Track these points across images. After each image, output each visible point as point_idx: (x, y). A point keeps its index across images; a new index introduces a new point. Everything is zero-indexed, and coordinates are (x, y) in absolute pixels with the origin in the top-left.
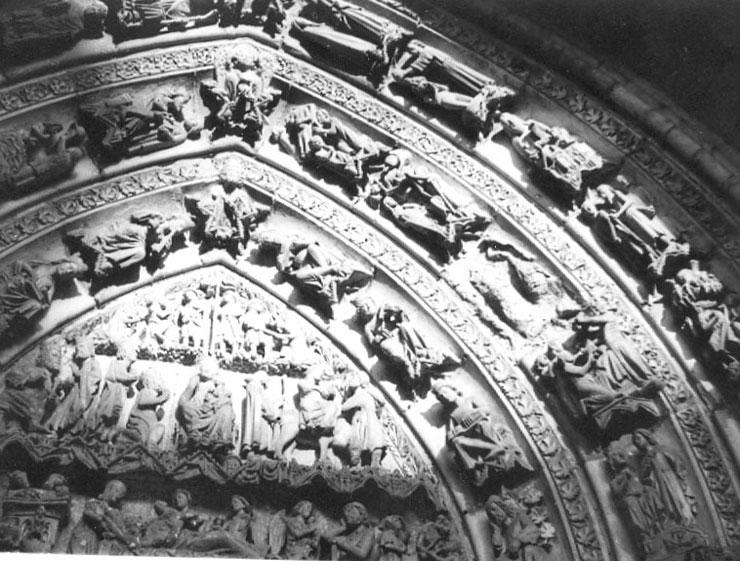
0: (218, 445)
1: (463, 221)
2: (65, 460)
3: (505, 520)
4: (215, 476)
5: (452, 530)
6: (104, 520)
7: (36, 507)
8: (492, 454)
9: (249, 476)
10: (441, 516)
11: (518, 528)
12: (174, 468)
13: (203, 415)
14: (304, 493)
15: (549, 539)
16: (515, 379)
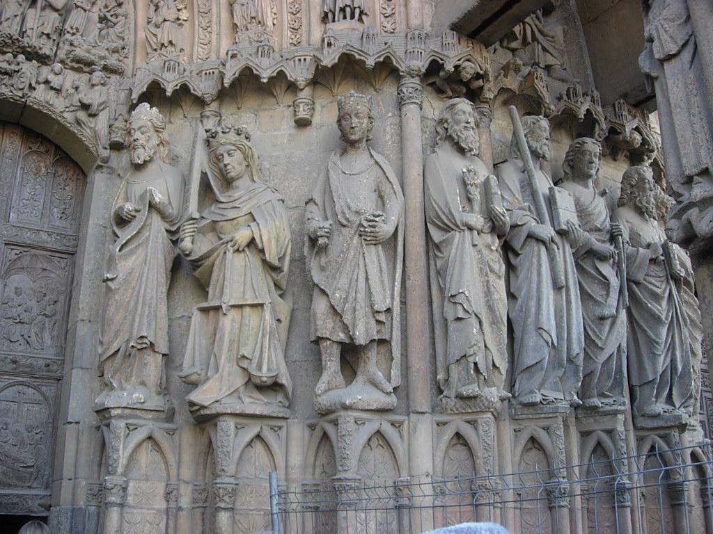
11: (165, 9)
15: (184, 20)
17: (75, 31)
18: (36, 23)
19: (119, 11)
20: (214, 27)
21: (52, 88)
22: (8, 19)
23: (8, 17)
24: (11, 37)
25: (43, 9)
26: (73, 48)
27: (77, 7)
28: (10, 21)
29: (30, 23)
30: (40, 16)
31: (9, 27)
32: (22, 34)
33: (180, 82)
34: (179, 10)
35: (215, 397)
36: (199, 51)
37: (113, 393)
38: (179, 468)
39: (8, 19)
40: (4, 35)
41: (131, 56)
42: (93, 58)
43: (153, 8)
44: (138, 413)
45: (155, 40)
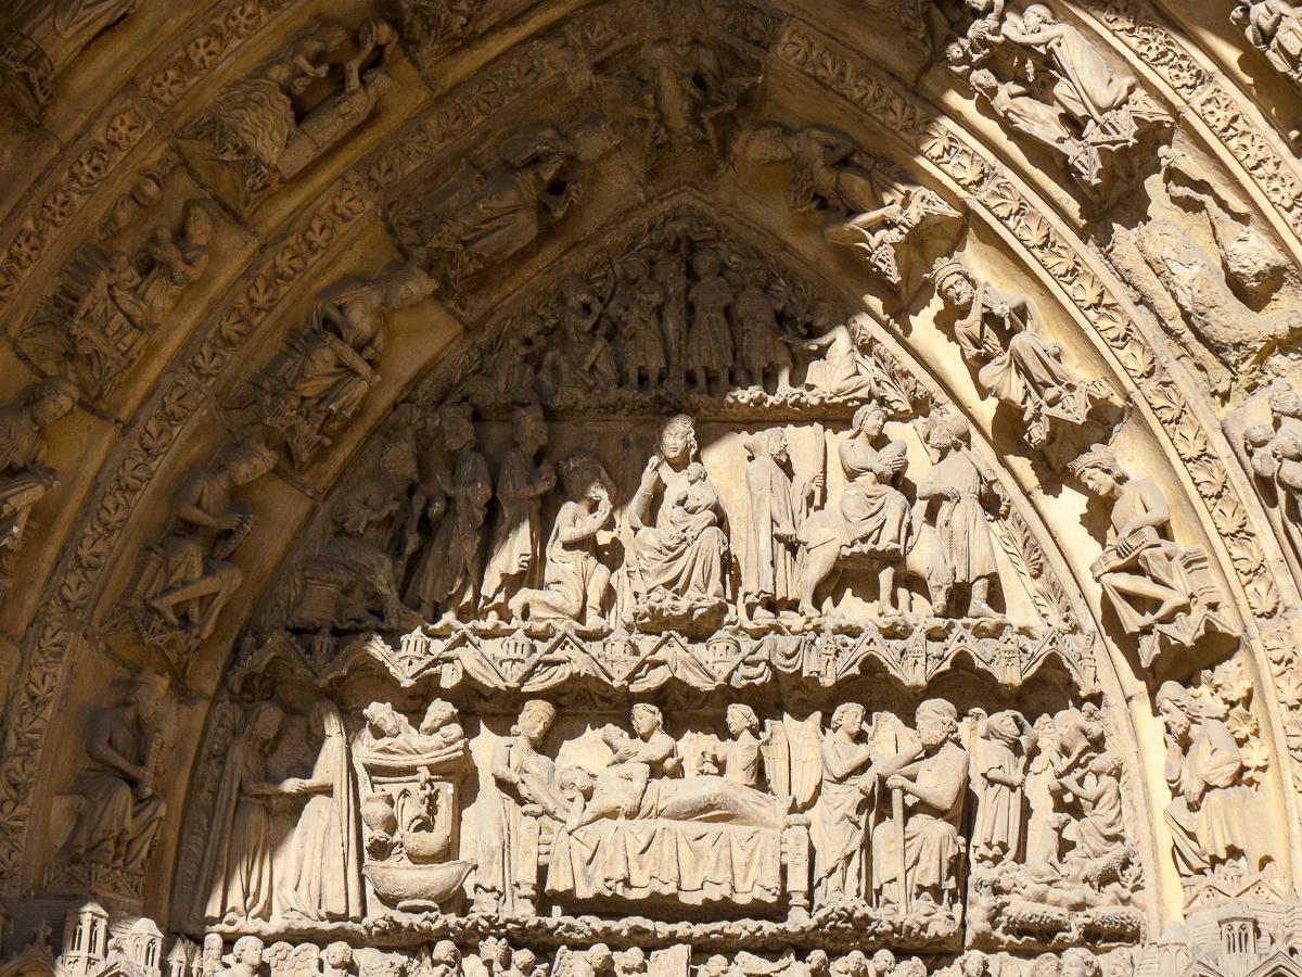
0: (700, 611)
1: (1113, 143)
2: (449, 678)
3: (1188, 729)
4: (695, 680)
5: (1111, 728)
6: (523, 782)
7: (412, 770)
8: (1162, 611)
9: (752, 671)
10: (1089, 706)
12: (627, 672)
13: (672, 555)
14: (846, 690)
16: (1211, 457)
17: (997, 850)
18: (900, 862)
19: (1099, 762)
22: (834, 870)
23: (831, 865)
24: (851, 915)
25: (909, 812)
26: (1004, 898)
27: (992, 782)
28: (837, 875)
29: (887, 864)
30: (905, 840)
31: (838, 889)
32: (872, 895)
34: (1241, 743)
39: (834, 870)
40: (834, 915)
41: (1149, 880)
42: (1053, 913)
43: (1179, 749)
45: (1194, 845)
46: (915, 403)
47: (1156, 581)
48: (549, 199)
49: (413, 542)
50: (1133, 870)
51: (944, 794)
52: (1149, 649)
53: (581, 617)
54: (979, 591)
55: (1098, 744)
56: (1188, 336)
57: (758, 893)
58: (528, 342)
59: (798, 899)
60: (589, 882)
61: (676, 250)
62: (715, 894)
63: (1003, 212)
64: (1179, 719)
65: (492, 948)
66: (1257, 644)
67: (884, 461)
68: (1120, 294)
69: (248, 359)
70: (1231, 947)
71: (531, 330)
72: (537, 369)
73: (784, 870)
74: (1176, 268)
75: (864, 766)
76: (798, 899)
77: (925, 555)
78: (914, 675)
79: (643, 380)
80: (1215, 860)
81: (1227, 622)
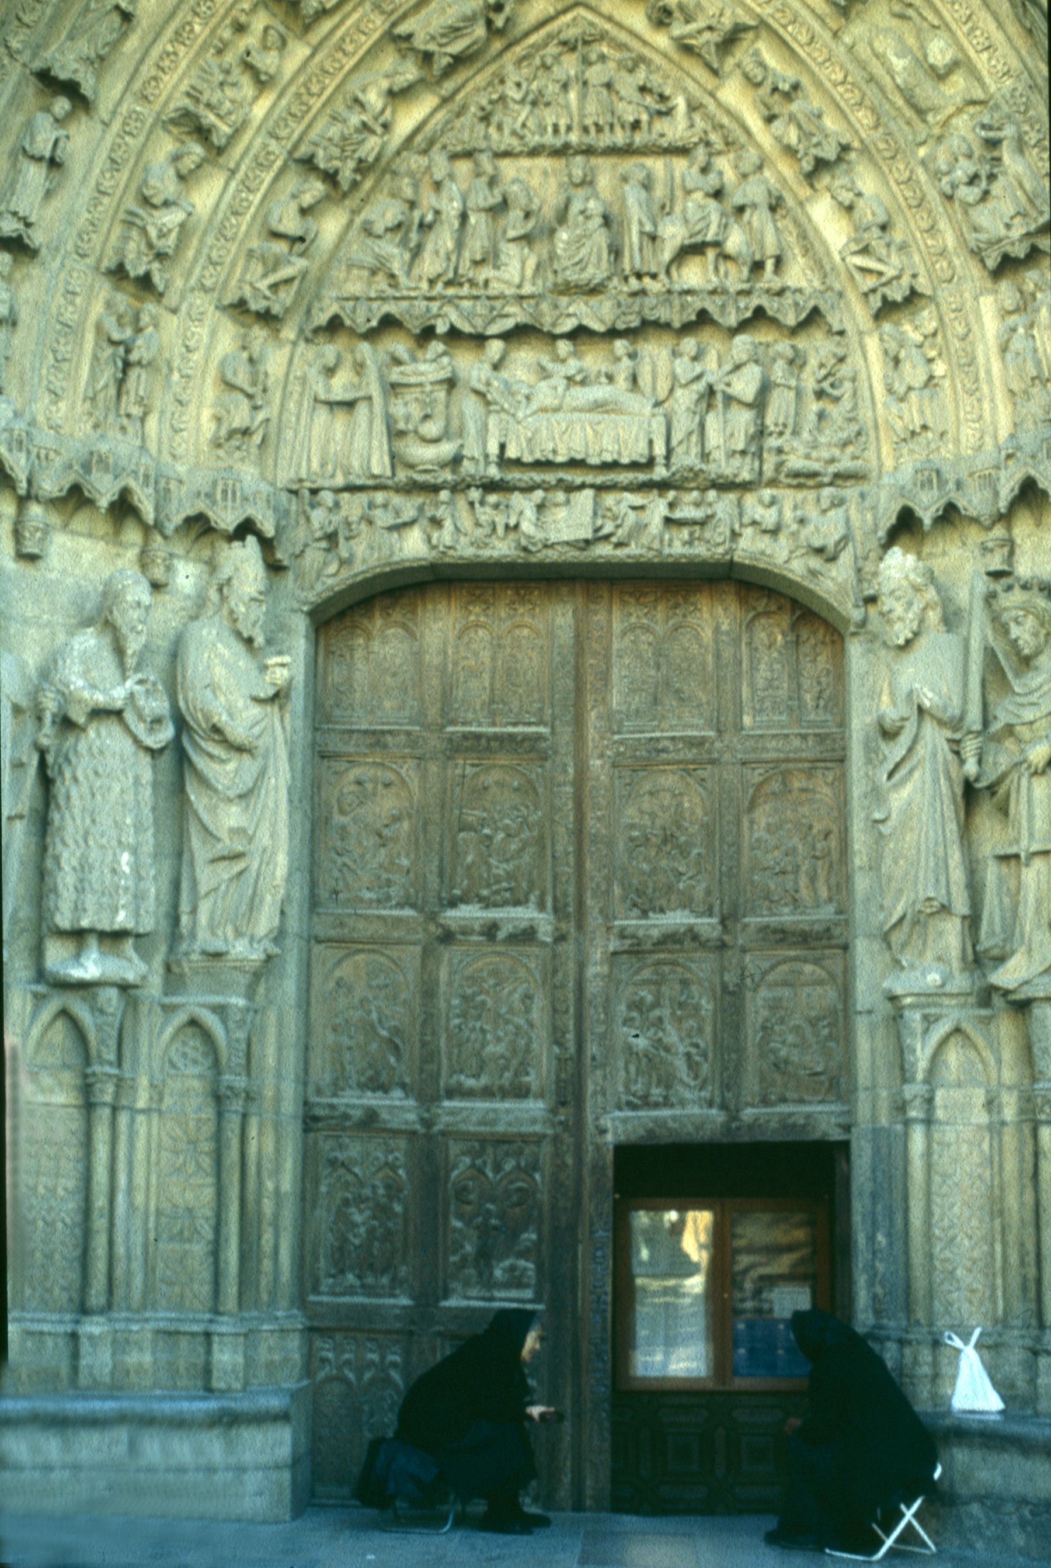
7: (421, 385)
8: (884, 279)
10: (837, 338)
20: (985, 388)
21: (765, 532)
26: (784, 457)
29: (714, 437)
32: (705, 456)
33: (943, 502)
34: (930, 361)
35: (1023, 974)
36: (968, 435)
37: (903, 976)
38: (999, 1070)
42: (816, 466)
43: (891, 364)
44: (936, 999)
46: (727, 144)
47: (880, 260)
48: (492, 15)
49: (414, 236)
50: (863, 439)
51: (749, 395)
52: (876, 302)
53: (519, 286)
54: (770, 265)
55: (842, 360)
56: (900, 102)
57: (636, 457)
58: (483, 109)
59: (660, 460)
60: (532, 452)
61: (573, 49)
62: (608, 458)
63: (784, 21)
64: (892, 346)
65: (475, 494)
66: (941, 300)
67: (712, 180)
68: (857, 75)
69: (309, 126)
70: (923, 486)
71: (484, 102)
72: (488, 125)
73: (651, 442)
74: (894, 60)
75: (699, 377)
76: (660, 460)
77: (735, 241)
78: (732, 320)
79: (556, 129)
80: (913, 433)
81: (923, 285)
